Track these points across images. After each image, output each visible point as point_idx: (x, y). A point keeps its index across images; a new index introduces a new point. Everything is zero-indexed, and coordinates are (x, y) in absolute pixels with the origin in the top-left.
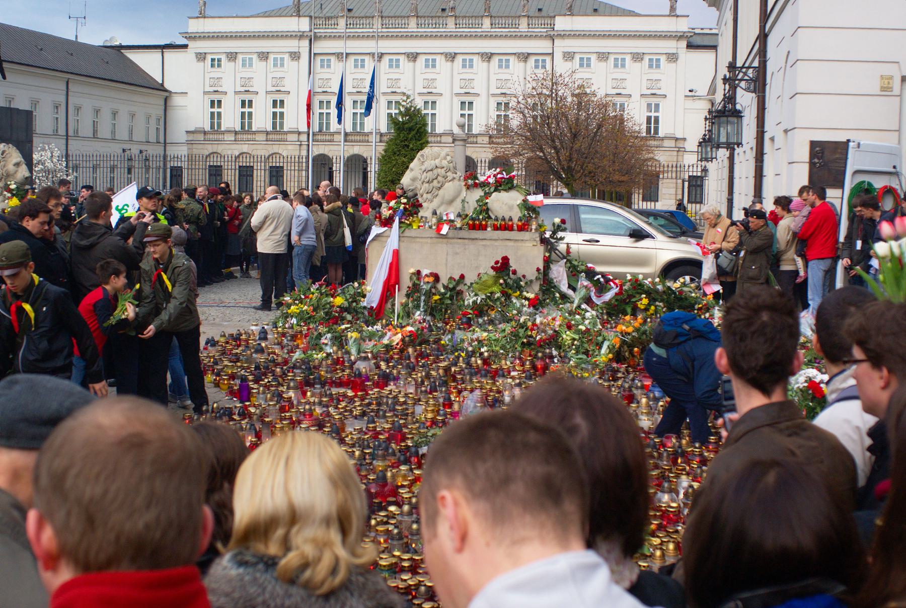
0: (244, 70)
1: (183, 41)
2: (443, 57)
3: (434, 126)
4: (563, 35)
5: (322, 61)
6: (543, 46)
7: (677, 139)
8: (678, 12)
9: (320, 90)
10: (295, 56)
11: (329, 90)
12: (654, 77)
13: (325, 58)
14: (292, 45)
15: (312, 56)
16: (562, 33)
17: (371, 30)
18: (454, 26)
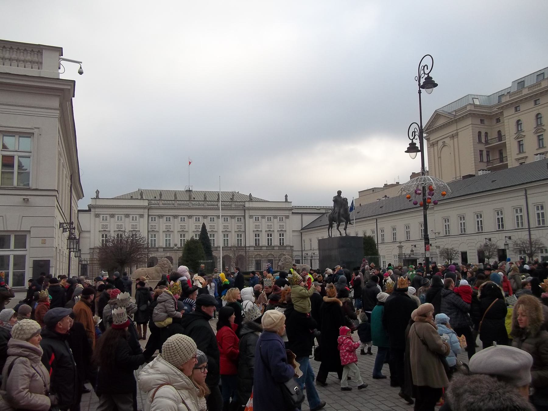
0: (103, 221)
1: (87, 209)
2: (203, 218)
3: (213, 244)
4: (250, 209)
5: (152, 218)
6: (239, 213)
7: (291, 246)
8: (288, 201)
9: (151, 230)
10: (142, 216)
11: (155, 230)
12: (281, 224)
13: (154, 217)
14: (141, 211)
15: (149, 215)
16: (250, 208)
17: (173, 206)
18: (207, 205)
